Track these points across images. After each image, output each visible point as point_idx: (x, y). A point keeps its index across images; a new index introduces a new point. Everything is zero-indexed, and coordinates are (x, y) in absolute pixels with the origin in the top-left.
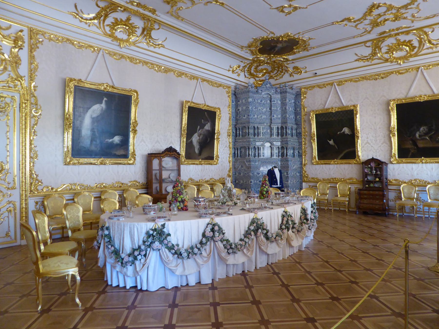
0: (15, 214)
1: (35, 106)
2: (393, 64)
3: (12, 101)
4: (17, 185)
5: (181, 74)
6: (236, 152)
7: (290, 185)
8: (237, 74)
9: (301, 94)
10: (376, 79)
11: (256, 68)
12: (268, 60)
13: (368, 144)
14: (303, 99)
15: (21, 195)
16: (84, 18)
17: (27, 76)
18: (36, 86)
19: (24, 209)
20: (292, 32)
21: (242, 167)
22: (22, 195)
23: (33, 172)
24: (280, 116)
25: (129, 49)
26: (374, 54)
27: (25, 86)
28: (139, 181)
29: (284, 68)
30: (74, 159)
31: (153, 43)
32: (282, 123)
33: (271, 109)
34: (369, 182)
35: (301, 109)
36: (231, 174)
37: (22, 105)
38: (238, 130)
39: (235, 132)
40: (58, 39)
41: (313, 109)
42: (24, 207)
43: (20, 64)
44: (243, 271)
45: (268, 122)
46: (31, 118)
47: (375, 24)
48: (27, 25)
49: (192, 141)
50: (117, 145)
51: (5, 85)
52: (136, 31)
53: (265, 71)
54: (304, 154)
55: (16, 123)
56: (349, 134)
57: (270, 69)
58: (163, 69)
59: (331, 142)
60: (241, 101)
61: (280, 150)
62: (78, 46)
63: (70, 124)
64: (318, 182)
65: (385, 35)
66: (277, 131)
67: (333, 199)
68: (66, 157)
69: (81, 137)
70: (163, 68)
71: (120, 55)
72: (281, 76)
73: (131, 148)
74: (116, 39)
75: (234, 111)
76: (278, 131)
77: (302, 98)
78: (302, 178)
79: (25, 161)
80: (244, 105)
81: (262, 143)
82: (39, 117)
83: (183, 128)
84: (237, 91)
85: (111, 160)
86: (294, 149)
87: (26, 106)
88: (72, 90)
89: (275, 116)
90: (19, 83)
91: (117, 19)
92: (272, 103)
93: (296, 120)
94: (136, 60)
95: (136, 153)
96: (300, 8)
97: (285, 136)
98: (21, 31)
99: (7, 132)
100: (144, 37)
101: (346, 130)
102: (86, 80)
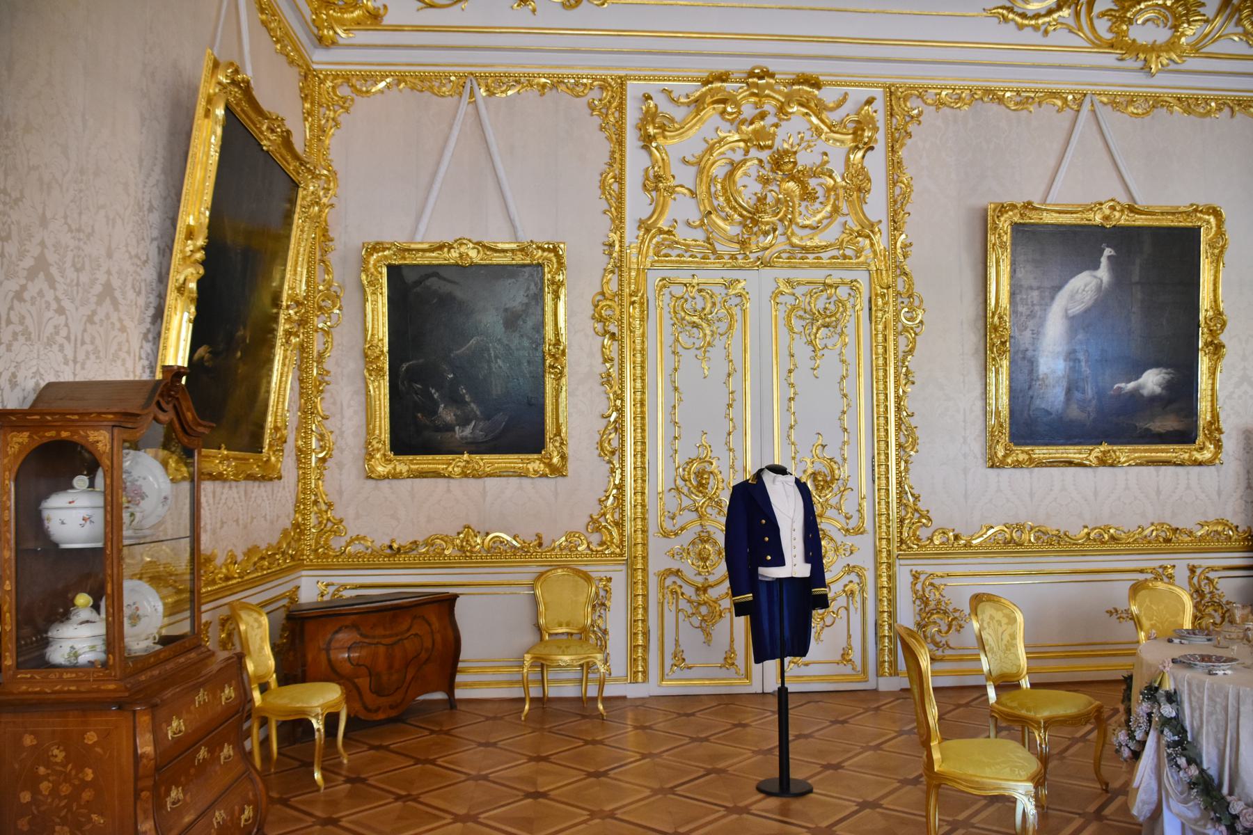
1: (906, 301)
4: (868, 524)
15: (877, 553)
16: (1029, 14)
17: (884, 218)
19: (885, 591)
40: (960, 98)
42: (885, 584)
43: (868, 191)
48: (883, 80)
50: (1153, 399)
51: (835, 253)
55: (862, 352)
63: (1003, 343)
69: (1038, 379)
73: (1204, 406)
74: (1133, 49)
79: (887, 455)
82: (917, 330)
85: (1135, 451)
88: (1007, 238)
90: (867, 241)
94: (1206, 101)
95: (1222, 425)
98: (869, 102)
99: (843, 378)
100: (1230, 17)
102: (1044, 203)
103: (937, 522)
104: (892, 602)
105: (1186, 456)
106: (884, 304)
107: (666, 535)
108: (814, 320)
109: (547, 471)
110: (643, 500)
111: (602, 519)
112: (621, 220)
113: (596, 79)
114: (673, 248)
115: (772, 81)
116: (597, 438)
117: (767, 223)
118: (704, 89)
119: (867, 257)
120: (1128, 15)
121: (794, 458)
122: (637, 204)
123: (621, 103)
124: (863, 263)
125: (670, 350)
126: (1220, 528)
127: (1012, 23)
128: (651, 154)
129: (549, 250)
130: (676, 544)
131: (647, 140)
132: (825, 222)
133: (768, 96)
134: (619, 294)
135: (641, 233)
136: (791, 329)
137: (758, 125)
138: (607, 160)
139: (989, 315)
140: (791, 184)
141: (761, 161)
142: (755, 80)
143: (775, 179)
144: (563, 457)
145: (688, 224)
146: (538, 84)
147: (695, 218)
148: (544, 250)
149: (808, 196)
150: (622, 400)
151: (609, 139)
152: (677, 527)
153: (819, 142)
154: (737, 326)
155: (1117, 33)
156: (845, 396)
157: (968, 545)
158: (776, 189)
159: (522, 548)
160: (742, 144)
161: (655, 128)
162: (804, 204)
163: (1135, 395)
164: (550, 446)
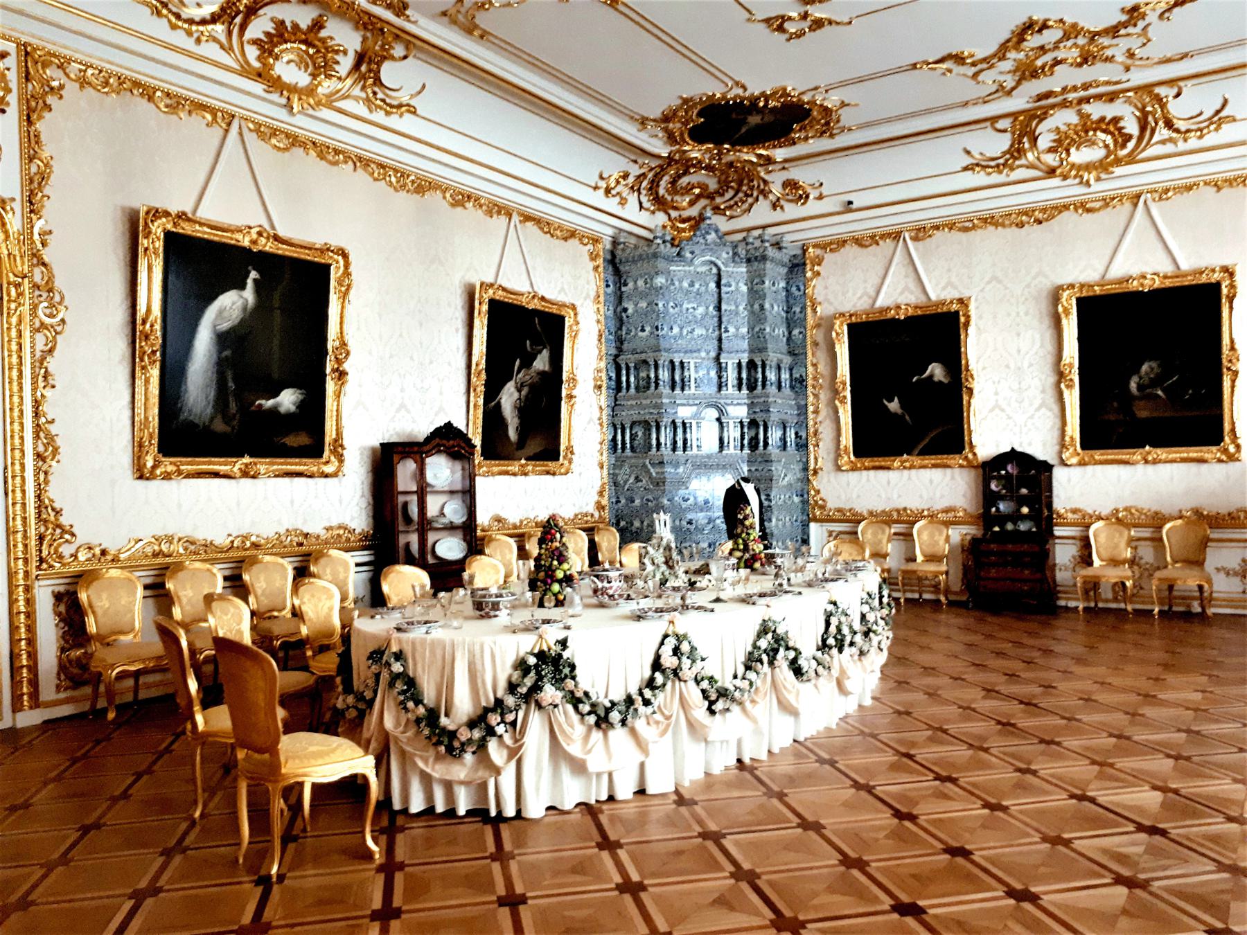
1: (45, 295)
2: (1069, 181)
5: (462, 199)
6: (619, 437)
7: (775, 532)
8: (617, 199)
9: (804, 264)
10: (1021, 225)
11: (673, 182)
12: (711, 159)
13: (997, 411)
14: (812, 279)
16: (184, 16)
17: (18, 198)
18: (47, 228)
19: (22, 616)
20: (796, 85)
21: (637, 479)
23: (47, 502)
24: (744, 330)
25: (311, 116)
26: (1016, 152)
28: (352, 525)
29: (755, 183)
30: (167, 460)
31: (383, 100)
32: (751, 351)
33: (719, 308)
34: (1002, 519)
35: (804, 309)
36: (605, 502)
37: (8, 289)
38: (624, 372)
39: (613, 375)
40: (106, 83)
41: (843, 310)
42: (22, 609)
44: (739, 761)
45: (710, 348)
47: (1028, 72)
48: (17, 35)
49: (499, 403)
50: (289, 416)
52: (337, 63)
53: (697, 191)
54: (812, 441)
56: (945, 381)
57: (713, 184)
58: (413, 182)
59: (894, 406)
60: (631, 285)
61: (746, 430)
62: (167, 106)
63: (154, 352)
64: (859, 522)
65: (1051, 101)
66: (735, 374)
67: (903, 568)
69: (186, 391)
70: (412, 178)
71: (288, 136)
72: (746, 206)
74: (276, 84)
75: (610, 313)
76: (740, 373)
77: (809, 274)
78: (810, 510)
79: (23, 465)
80: (643, 296)
81: (695, 408)
82: (59, 329)
83: (474, 367)
84: (619, 252)
85: (273, 464)
86: (785, 428)
87: (20, 295)
88: (160, 245)
89: (732, 330)
91: (283, 22)
92: (724, 289)
93: (788, 340)
94: (337, 152)
95: (345, 443)
96: (830, 23)
97: (760, 387)
101: (936, 371)
104: (31, 629)
105: (315, 469)
120: (276, 50)
126: (341, 532)
139: (139, 321)
155: (264, 65)
163: (274, 411)
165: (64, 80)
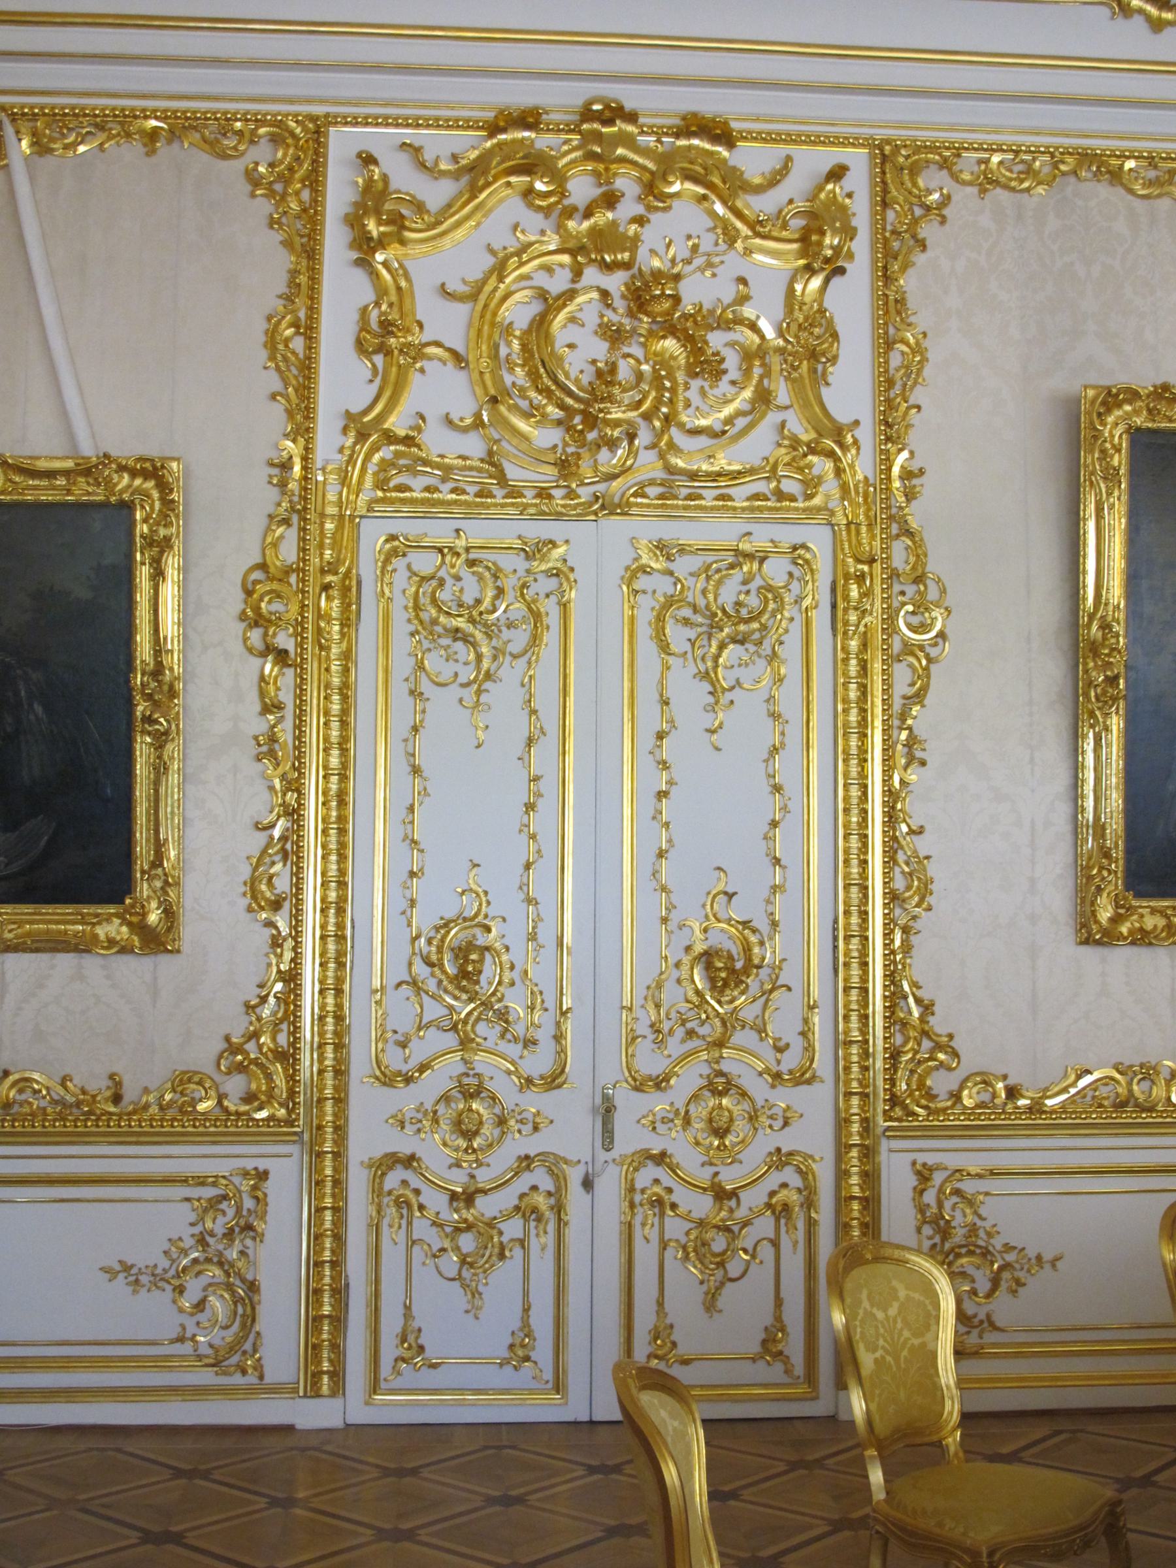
0: (811, 1224)
1: (911, 590)
3: (797, 573)
4: (822, 1063)
15: (841, 1123)
18: (915, 466)
19: (856, 1206)
22: (847, 1121)
27: (860, 476)
40: (1029, 171)
43: (834, 360)
46: (890, 659)
51: (761, 487)
63: (1112, 681)
68: (1085, 891)
82: (933, 652)
87: (866, 594)
90: (829, 465)
98: (837, 173)
99: (774, 750)
103: (971, 1061)
106: (863, 595)
107: (387, 1079)
108: (715, 627)
109: (136, 940)
110: (339, 1006)
111: (251, 1046)
112: (308, 412)
113: (261, 123)
114: (416, 473)
115: (630, 128)
116: (246, 872)
117: (617, 423)
118: (489, 144)
119: (828, 496)
121: (665, 920)
122: (343, 381)
123: (315, 170)
124: (818, 509)
125: (405, 688)
127: (1138, 20)
128: (374, 274)
129: (146, 475)
130: (406, 1099)
131: (365, 246)
132: (741, 422)
133: (623, 160)
134: (300, 569)
135: (349, 442)
136: (664, 647)
137: (602, 218)
138: (283, 289)
140: (670, 345)
141: (605, 294)
142: (597, 126)
143: (634, 331)
144: (169, 913)
145: (449, 422)
146: (142, 132)
147: (464, 407)
148: (134, 474)
149: (706, 366)
150: (298, 791)
151: (287, 244)
152: (413, 1063)
153: (731, 258)
154: (551, 638)
156: (777, 788)
157: (1036, 1108)
158: (638, 352)
159: (78, 1104)
160: (566, 258)
161: (380, 223)
162: (696, 384)
164: (144, 889)
165: (949, 186)
